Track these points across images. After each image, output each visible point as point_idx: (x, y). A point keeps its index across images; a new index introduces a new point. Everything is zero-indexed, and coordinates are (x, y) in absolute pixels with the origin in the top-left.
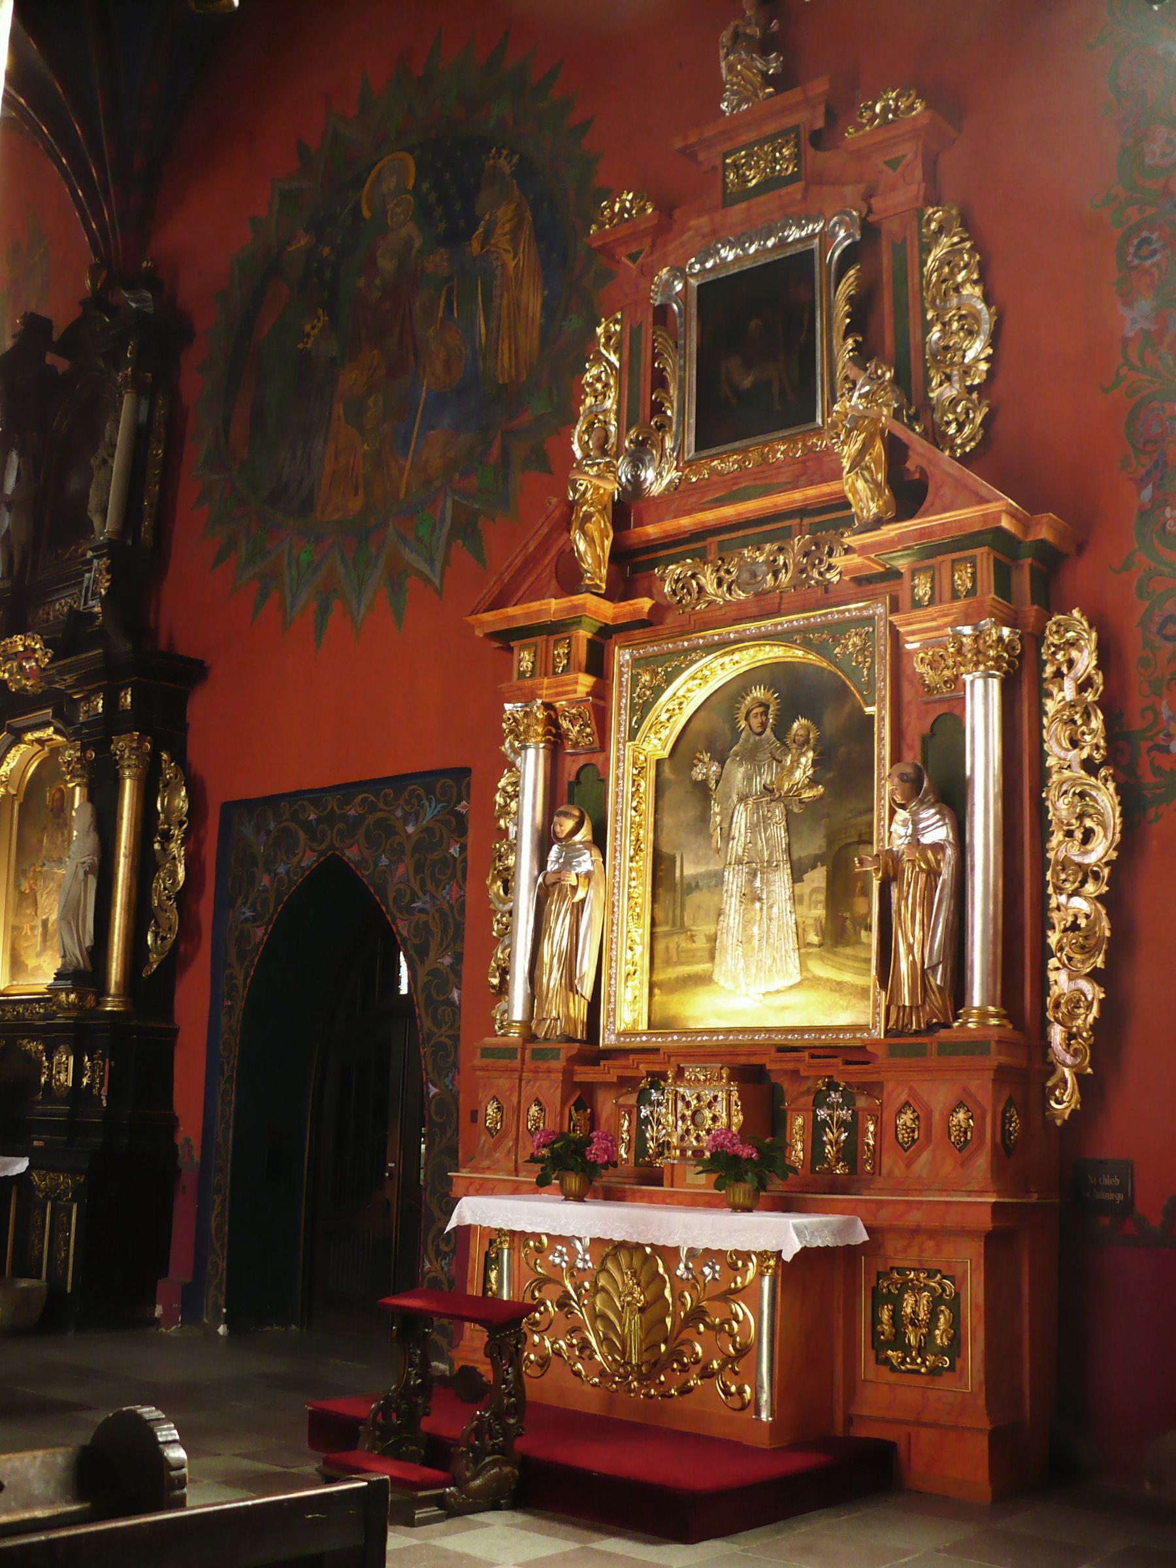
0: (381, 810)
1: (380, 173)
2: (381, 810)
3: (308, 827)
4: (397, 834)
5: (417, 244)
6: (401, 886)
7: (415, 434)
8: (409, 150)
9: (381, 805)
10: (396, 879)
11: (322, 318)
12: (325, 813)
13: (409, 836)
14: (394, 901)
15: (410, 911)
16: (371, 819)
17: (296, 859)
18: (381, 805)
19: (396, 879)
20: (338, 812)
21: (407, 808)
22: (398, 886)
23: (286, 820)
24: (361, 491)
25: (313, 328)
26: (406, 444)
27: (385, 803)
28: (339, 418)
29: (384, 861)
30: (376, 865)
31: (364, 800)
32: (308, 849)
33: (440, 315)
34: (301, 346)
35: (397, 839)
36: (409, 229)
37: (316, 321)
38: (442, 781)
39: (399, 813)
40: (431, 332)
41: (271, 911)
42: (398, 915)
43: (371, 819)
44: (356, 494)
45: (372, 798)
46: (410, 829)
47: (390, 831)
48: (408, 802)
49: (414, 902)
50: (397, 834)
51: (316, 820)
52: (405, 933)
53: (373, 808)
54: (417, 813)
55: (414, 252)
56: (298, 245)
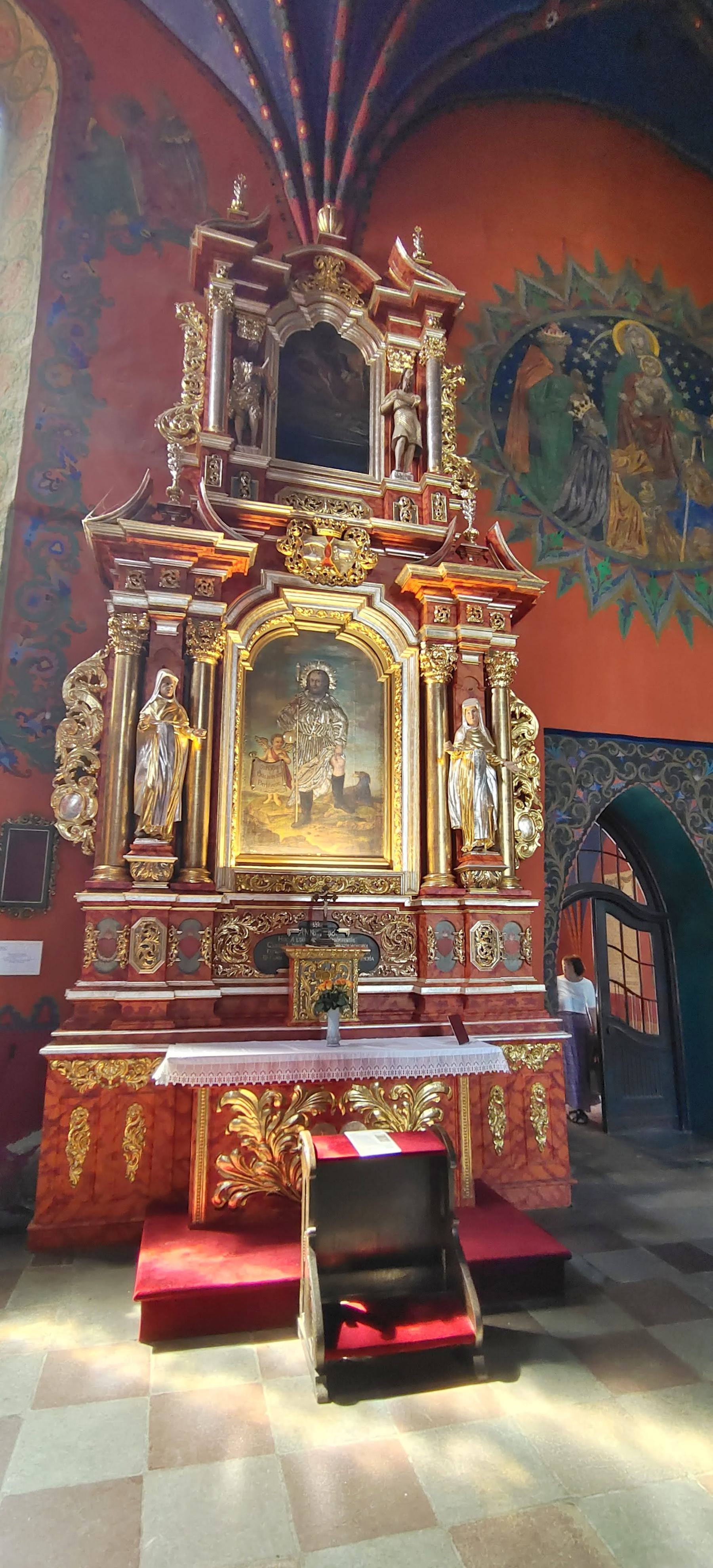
0: (675, 761)
1: (626, 328)
2: (675, 761)
3: (616, 760)
4: (688, 779)
5: (669, 396)
6: (696, 815)
7: (685, 523)
8: (653, 329)
9: (675, 757)
10: (691, 810)
11: (589, 403)
12: (631, 755)
13: (696, 782)
14: (691, 825)
15: (703, 832)
16: (669, 766)
17: (607, 783)
18: (675, 757)
19: (691, 810)
20: (642, 756)
21: (694, 764)
22: (693, 814)
23: (596, 753)
24: (645, 543)
25: (583, 406)
26: (679, 525)
27: (678, 757)
28: (617, 484)
29: (681, 796)
30: (676, 797)
31: (661, 752)
32: (617, 778)
33: (693, 453)
34: (571, 412)
35: (689, 783)
36: (660, 383)
37: (583, 402)
38: (695, 752)
39: (688, 766)
40: (686, 461)
41: (588, 817)
42: (696, 834)
43: (669, 766)
44: (640, 542)
45: (668, 752)
46: (697, 778)
47: (683, 777)
48: (694, 760)
49: (705, 826)
50: (688, 779)
51: (624, 757)
52: (701, 846)
53: (669, 759)
54: (701, 770)
55: (666, 401)
56: (553, 335)
